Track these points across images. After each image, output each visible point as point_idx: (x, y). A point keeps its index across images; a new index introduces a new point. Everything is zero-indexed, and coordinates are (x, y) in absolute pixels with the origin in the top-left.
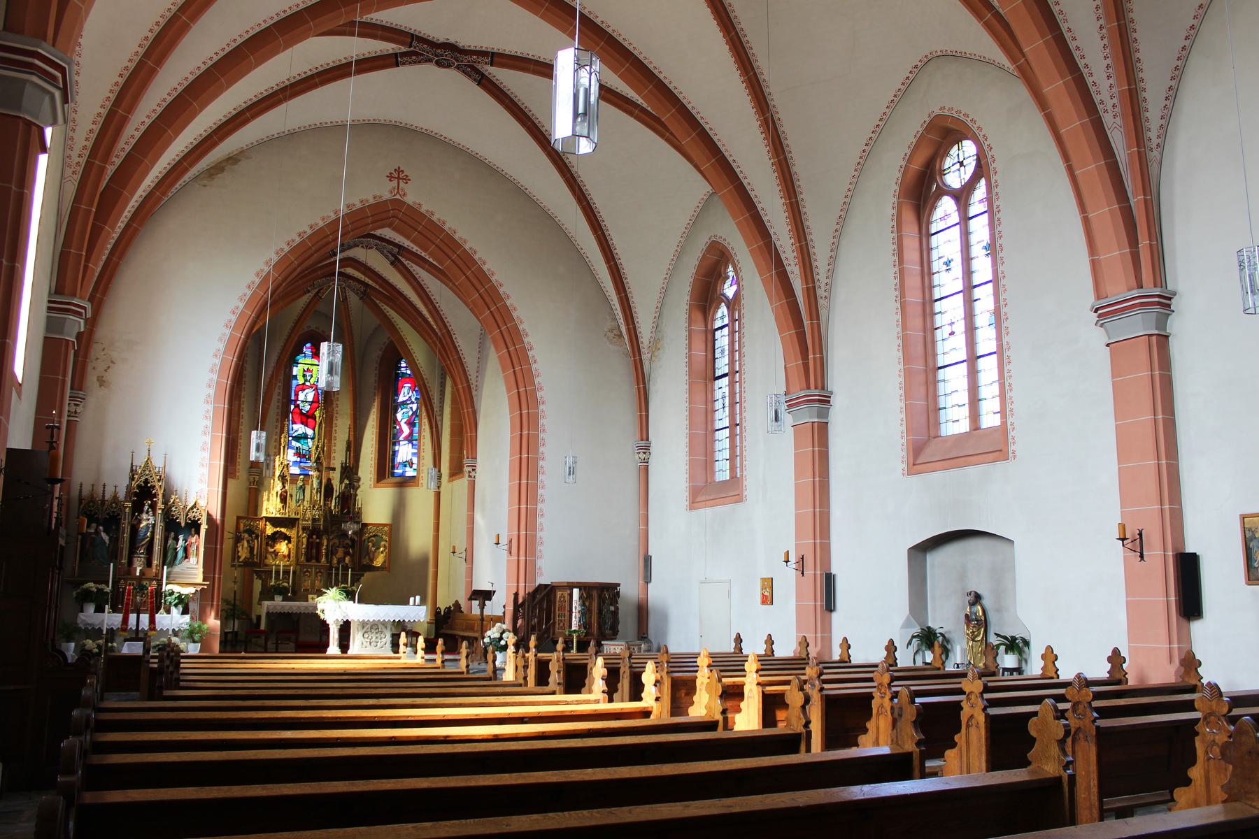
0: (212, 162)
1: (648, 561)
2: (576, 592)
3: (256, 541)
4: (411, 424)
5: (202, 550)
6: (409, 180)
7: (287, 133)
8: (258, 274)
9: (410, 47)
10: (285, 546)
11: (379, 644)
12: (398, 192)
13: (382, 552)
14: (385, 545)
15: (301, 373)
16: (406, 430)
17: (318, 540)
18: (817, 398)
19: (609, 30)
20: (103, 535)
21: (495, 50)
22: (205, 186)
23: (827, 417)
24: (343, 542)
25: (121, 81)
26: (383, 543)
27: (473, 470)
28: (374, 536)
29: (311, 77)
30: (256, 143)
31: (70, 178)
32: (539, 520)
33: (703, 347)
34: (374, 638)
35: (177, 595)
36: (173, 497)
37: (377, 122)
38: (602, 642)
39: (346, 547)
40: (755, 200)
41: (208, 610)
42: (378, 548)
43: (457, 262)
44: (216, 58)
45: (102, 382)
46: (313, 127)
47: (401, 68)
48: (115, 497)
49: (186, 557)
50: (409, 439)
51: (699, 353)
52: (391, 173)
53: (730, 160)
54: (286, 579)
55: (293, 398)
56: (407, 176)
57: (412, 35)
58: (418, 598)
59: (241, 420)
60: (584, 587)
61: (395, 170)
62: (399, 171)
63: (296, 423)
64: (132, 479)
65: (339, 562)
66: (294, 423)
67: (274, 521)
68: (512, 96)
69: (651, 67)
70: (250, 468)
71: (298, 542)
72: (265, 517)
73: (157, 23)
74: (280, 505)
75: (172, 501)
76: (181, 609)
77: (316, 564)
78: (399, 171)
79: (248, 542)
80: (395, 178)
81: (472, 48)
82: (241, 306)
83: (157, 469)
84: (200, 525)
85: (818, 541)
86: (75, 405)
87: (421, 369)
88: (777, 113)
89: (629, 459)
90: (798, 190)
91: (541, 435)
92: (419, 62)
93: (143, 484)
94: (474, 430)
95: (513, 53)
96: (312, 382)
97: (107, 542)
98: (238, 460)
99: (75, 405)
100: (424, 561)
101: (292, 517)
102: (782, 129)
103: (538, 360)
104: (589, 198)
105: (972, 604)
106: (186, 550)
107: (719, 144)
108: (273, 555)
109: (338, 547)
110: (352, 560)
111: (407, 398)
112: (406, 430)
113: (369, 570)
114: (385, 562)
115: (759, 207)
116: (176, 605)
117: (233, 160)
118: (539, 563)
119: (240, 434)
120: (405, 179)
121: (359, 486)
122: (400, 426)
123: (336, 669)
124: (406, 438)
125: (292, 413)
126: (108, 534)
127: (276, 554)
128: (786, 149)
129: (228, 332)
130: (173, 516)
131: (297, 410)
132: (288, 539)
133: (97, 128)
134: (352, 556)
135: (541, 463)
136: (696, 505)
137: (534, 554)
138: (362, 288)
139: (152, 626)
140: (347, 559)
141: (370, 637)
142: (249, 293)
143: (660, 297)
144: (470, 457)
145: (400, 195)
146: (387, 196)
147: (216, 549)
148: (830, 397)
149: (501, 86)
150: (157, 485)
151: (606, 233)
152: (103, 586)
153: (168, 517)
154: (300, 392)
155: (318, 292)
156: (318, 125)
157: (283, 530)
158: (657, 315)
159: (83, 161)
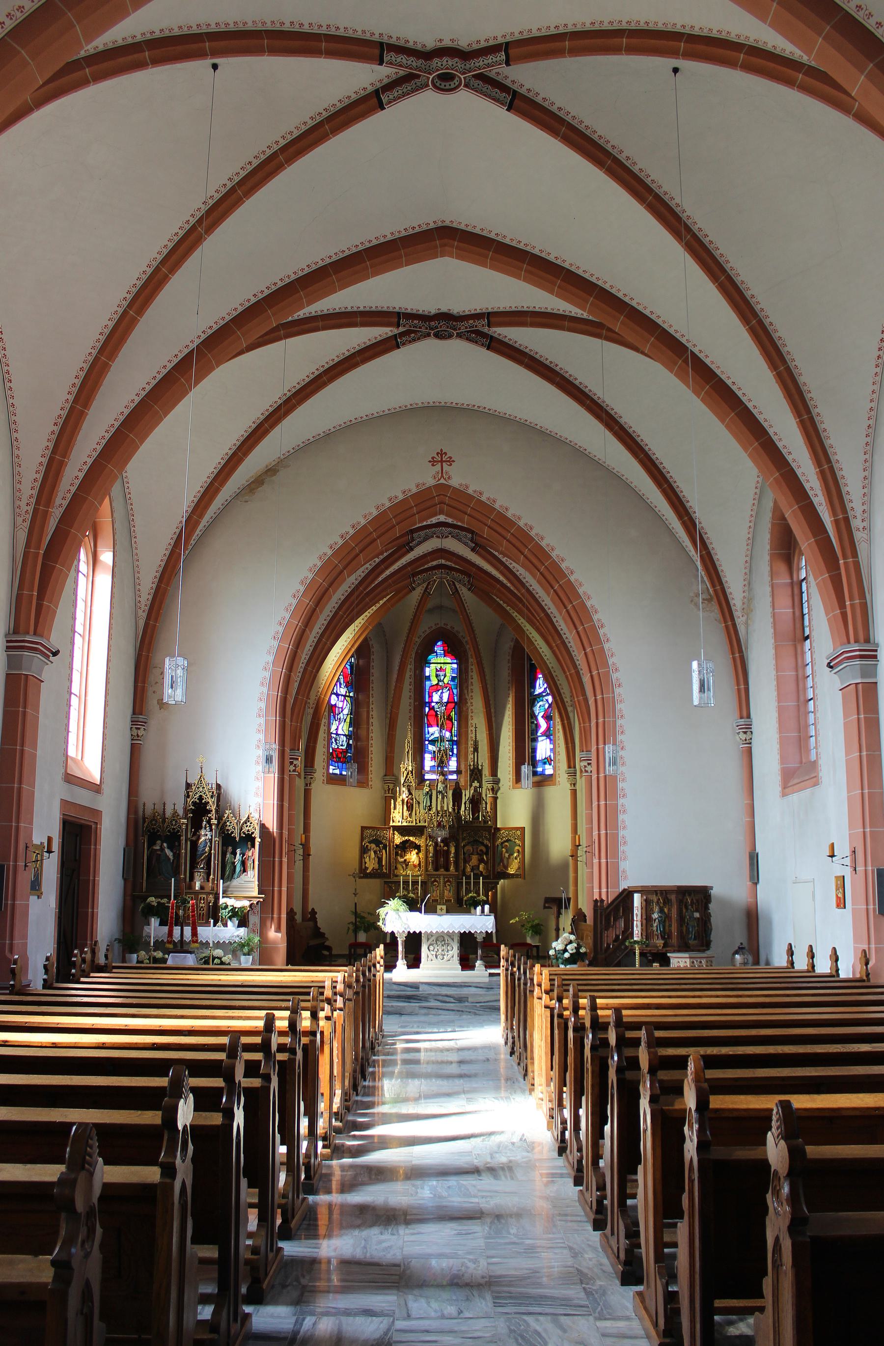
1: (754, 859)
2: (637, 897)
3: (384, 851)
4: (548, 718)
5: (257, 863)
6: (454, 461)
7: (322, 435)
8: (302, 583)
9: (398, 326)
10: (415, 855)
11: (445, 957)
12: (442, 476)
13: (516, 858)
16: (543, 724)
17: (445, 848)
18: (858, 653)
19: (566, 265)
20: (167, 851)
21: (490, 310)
23: (875, 676)
24: (477, 848)
25: (57, 429)
26: (517, 848)
27: (589, 764)
28: (508, 841)
29: (319, 376)
30: (292, 451)
31: (21, 526)
32: (621, 817)
33: (789, 602)
34: (440, 951)
35: (230, 908)
36: (227, 812)
37: (415, 406)
38: (668, 955)
39: (481, 854)
40: (765, 425)
41: (268, 923)
42: (512, 854)
44: (148, 388)
46: (349, 423)
47: (403, 350)
48: (175, 813)
49: (245, 871)
50: (547, 734)
51: (786, 611)
52: (433, 458)
53: (729, 382)
54: (415, 890)
55: (427, 700)
56: (450, 458)
57: (399, 313)
58: (487, 907)
59: (371, 728)
60: (643, 891)
61: (438, 454)
62: (441, 453)
65: (472, 870)
66: (430, 726)
67: (402, 830)
68: (532, 353)
69: (620, 295)
70: (385, 776)
71: (427, 851)
72: (392, 826)
73: (82, 369)
74: (406, 813)
75: (226, 815)
76: (237, 922)
77: (445, 873)
78: (441, 453)
79: (375, 852)
80: (438, 461)
81: (467, 313)
82: (288, 616)
83: (210, 785)
84: (254, 838)
85: (868, 830)
86: (137, 728)
87: (545, 658)
88: (767, 317)
89: (733, 741)
90: (811, 404)
91: (619, 722)
92: (419, 339)
93: (198, 801)
94: (587, 720)
95: (508, 309)
96: (446, 681)
97: (171, 857)
99: (137, 728)
100: (564, 866)
101: (419, 824)
102: (777, 335)
103: (611, 639)
104: (646, 448)
106: (243, 863)
107: (713, 367)
108: (404, 865)
109: (472, 854)
110: (486, 869)
112: (543, 724)
113: (504, 878)
114: (519, 868)
115: (771, 432)
116: (230, 918)
117: (271, 471)
118: (622, 865)
119: (371, 742)
120: (436, 461)
121: (499, 788)
122: (537, 720)
123: (263, 981)
124: (543, 734)
125: (427, 715)
126: (172, 851)
127: (406, 863)
128: (787, 358)
129: (275, 644)
130: (228, 830)
131: (432, 712)
132: (418, 847)
133: (40, 477)
134: (486, 863)
136: (787, 790)
138: (466, 579)
139: (195, 939)
140: (481, 867)
141: (436, 950)
142: (294, 602)
143: (748, 550)
145: (445, 479)
146: (431, 482)
147: (274, 861)
148: (876, 651)
149: (517, 345)
150: (210, 801)
151: (675, 485)
152: (165, 900)
153: (223, 832)
154: (434, 693)
155: (427, 588)
156: (354, 421)
157: (411, 838)
158: (747, 571)
159: (31, 509)
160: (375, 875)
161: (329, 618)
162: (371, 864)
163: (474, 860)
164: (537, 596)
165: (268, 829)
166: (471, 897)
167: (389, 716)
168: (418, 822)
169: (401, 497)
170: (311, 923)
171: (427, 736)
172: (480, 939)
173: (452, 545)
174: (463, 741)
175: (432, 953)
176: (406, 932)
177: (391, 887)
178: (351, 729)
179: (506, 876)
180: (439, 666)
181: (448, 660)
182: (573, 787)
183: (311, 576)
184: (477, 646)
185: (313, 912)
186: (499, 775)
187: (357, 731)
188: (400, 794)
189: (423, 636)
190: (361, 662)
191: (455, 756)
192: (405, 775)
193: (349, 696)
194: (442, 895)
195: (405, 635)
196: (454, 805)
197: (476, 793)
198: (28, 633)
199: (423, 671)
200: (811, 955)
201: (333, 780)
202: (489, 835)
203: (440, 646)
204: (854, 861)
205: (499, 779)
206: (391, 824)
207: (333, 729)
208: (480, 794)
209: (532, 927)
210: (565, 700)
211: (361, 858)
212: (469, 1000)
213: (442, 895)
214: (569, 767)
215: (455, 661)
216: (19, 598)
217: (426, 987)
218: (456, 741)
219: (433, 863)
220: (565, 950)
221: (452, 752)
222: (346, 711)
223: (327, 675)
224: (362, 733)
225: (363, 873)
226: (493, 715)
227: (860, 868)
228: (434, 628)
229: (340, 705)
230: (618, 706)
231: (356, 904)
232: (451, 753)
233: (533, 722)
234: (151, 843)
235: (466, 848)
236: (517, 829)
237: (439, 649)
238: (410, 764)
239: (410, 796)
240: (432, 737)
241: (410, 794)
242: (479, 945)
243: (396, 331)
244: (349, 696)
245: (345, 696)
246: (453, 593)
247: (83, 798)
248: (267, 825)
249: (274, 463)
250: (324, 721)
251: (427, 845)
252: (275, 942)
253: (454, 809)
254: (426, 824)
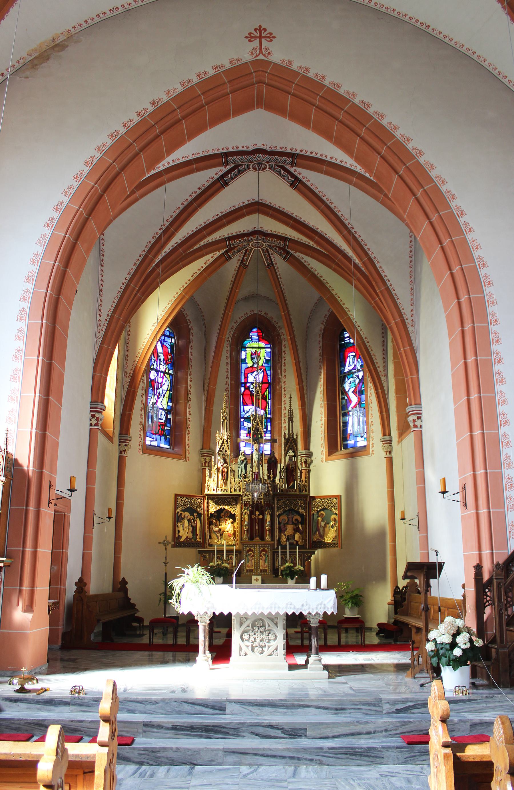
0: (35, 50)
3: (198, 520)
4: (359, 392)
6: (274, 37)
8: (87, 163)
10: (230, 524)
11: (265, 649)
13: (332, 527)
14: (335, 519)
15: (249, 357)
16: (354, 399)
17: (261, 517)
22: (27, 78)
24: (292, 518)
26: (333, 516)
27: (419, 418)
28: (323, 509)
34: (258, 640)
39: (296, 523)
42: (329, 523)
43: (347, 122)
52: (250, 34)
54: (229, 559)
55: (243, 381)
56: (271, 34)
58: (324, 578)
61: (256, 30)
62: (260, 29)
63: (247, 405)
65: (288, 539)
66: (245, 404)
67: (217, 499)
71: (242, 520)
72: (207, 495)
74: (221, 482)
78: (260, 29)
79: (189, 521)
80: (256, 37)
82: (66, 200)
91: (493, 328)
94: (415, 371)
96: (260, 364)
98: (187, 442)
100: (381, 535)
101: (234, 493)
103: (475, 228)
108: (219, 535)
109: (287, 523)
111: (352, 367)
112: (354, 399)
113: (320, 547)
114: (336, 537)
119: (188, 416)
121: (312, 462)
127: (221, 532)
129: (48, 232)
131: (247, 392)
132: (233, 516)
134: (301, 533)
135: (497, 367)
137: (500, 503)
140: (297, 536)
141: (252, 639)
142: (76, 184)
144: (413, 403)
145: (264, 55)
146: (247, 57)
147: (27, 511)
154: (249, 375)
157: (227, 508)
160: (189, 544)
161: (138, 263)
162: (185, 532)
163: (290, 529)
164: (359, 239)
165: (20, 466)
166: (288, 567)
167: (206, 392)
168: (233, 490)
169: (211, 72)
170: (121, 594)
171: (243, 413)
172: (314, 623)
174: (277, 418)
175: (247, 643)
176: (210, 615)
177: (204, 556)
178: (170, 404)
179: (321, 545)
180: (254, 350)
181: (262, 344)
182: (388, 455)
183: (98, 156)
184: (291, 323)
185: (124, 582)
186: (312, 449)
187: (175, 406)
188: (215, 464)
189: (239, 321)
190: (181, 342)
191: (268, 432)
192: (220, 444)
193: (168, 374)
194: (257, 565)
195: (222, 312)
196: (269, 473)
197: (291, 462)
199: (239, 354)
201: (149, 450)
202: (305, 504)
203: (255, 332)
205: (312, 453)
206: (206, 492)
207: (152, 400)
208: (295, 463)
209: (351, 598)
210: (379, 370)
211: (175, 526)
212: (309, 733)
213: (257, 565)
214: (384, 435)
215: (269, 346)
217: (237, 708)
218: (270, 418)
219: (248, 532)
220: (453, 645)
221: (267, 428)
222: (165, 387)
223: (145, 344)
224: (181, 407)
225: (177, 543)
226: (305, 392)
228: (249, 314)
230: (490, 309)
231: (166, 574)
232: (265, 430)
233: (344, 398)
235: (282, 517)
236: (334, 497)
237: (254, 335)
238: (226, 433)
239: (225, 465)
240: (247, 415)
241: (225, 462)
242: (313, 632)
243: (224, 170)
244: (168, 374)
245: (165, 373)
246: (269, 265)
248: (21, 461)
249: (62, 38)
250: (140, 392)
251: (242, 514)
252: (22, 627)
253: (269, 478)
254: (241, 493)
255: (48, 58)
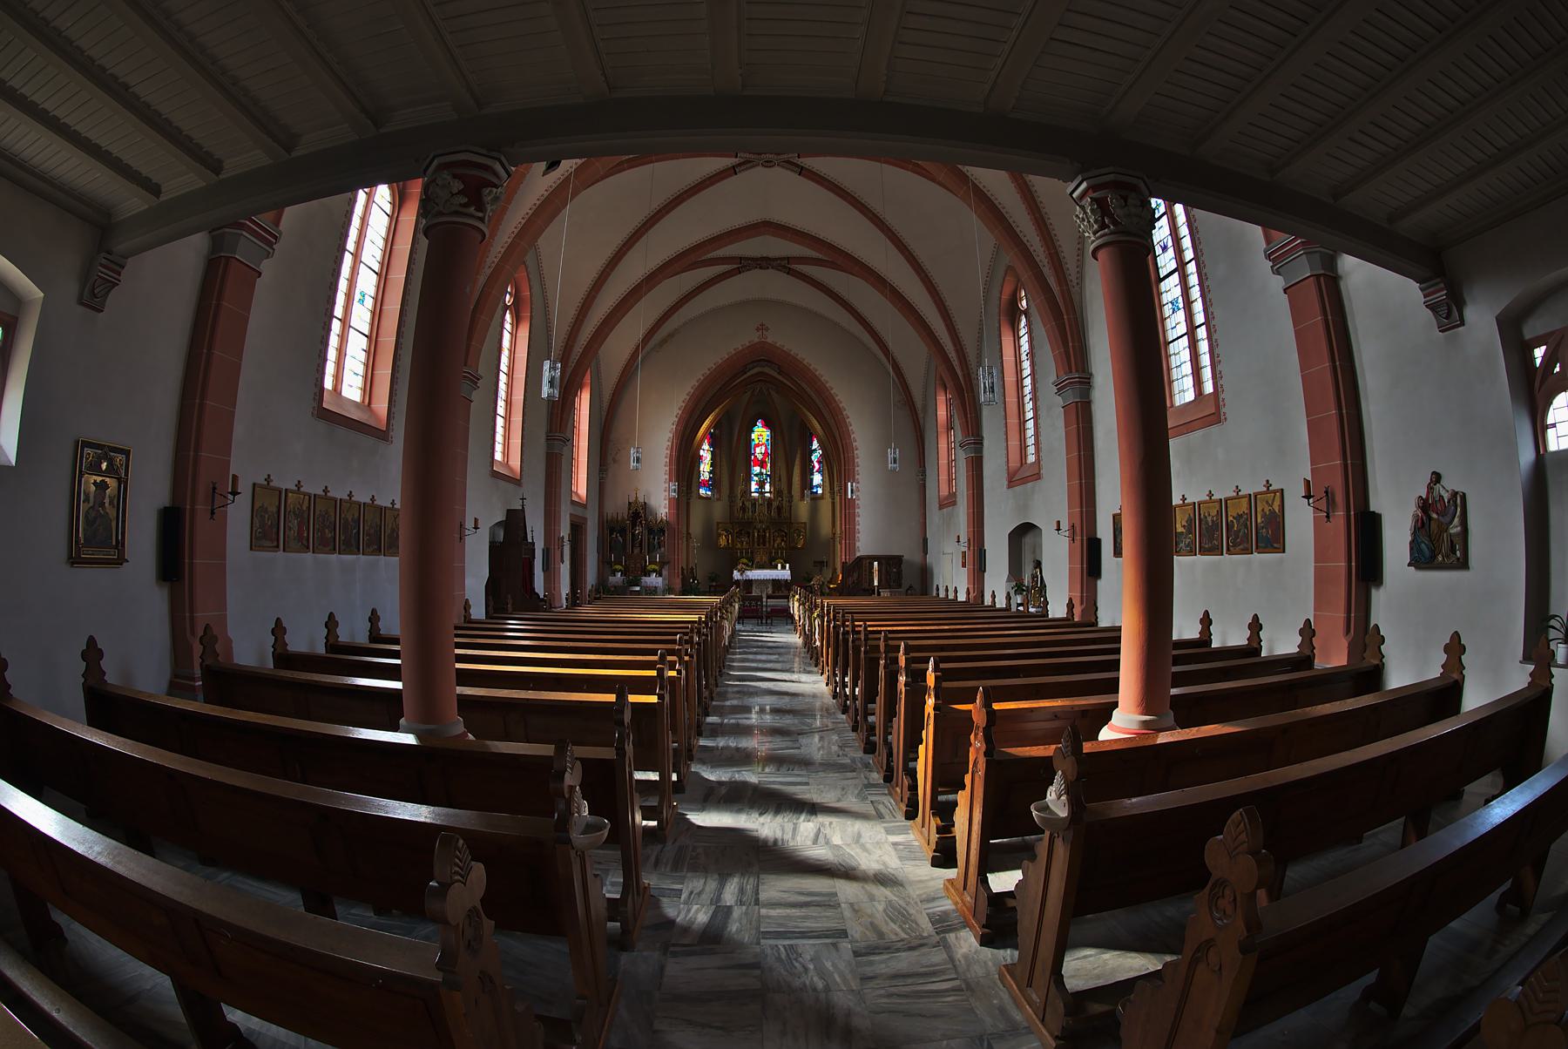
1: (925, 541)
4: (819, 462)
20: (620, 538)
39: (782, 536)
45: (615, 461)
48: (623, 517)
64: (629, 509)
105: (1036, 568)
117: (671, 336)
118: (858, 544)
134: (785, 542)
146: (757, 340)
163: (779, 540)
173: (767, 370)
181: (764, 430)
186: (793, 493)
198: (556, 432)
200: (947, 590)
204: (969, 544)
207: (701, 469)
208: (782, 504)
216: (552, 413)
227: (972, 548)
229: (705, 455)
234: (611, 534)
237: (759, 424)
247: (579, 512)
255: (666, 342)
